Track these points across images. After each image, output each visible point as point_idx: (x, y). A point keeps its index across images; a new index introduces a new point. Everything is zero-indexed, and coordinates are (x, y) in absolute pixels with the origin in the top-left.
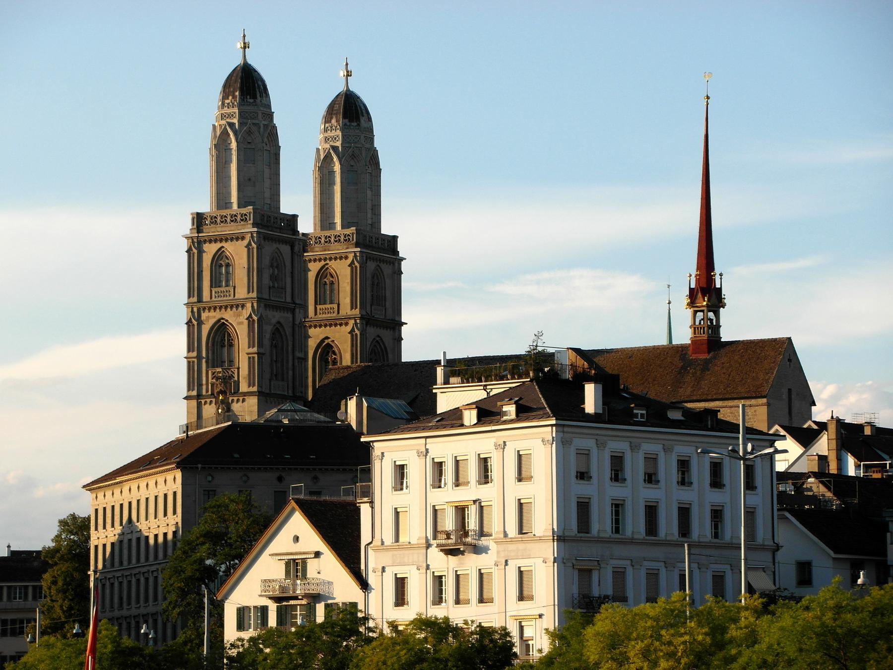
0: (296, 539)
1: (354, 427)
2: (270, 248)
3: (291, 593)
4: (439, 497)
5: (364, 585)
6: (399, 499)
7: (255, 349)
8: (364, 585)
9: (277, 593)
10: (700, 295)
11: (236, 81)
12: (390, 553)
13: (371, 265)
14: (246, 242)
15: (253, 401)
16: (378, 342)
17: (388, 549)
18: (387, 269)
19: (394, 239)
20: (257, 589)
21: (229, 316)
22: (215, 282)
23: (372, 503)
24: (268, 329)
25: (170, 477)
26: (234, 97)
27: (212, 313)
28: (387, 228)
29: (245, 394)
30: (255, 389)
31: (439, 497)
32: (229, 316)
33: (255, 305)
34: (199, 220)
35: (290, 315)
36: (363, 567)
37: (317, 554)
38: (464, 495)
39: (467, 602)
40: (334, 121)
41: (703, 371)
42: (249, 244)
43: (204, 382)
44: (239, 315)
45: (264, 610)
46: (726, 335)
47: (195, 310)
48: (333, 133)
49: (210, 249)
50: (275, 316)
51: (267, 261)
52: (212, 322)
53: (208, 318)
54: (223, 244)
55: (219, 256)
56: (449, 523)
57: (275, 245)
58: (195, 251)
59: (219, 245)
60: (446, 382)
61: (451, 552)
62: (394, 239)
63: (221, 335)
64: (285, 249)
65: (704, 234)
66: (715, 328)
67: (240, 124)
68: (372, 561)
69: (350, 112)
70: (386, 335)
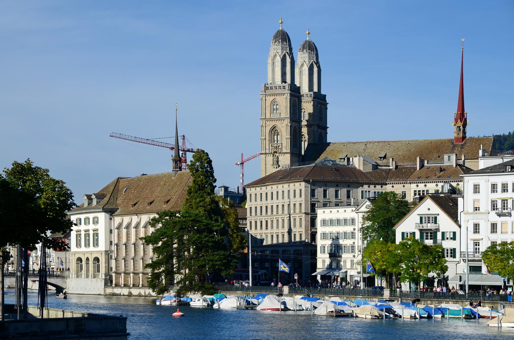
0: (429, 209)
1: (358, 168)
2: (294, 98)
3: (425, 228)
4: (494, 196)
5: (460, 226)
6: (477, 196)
7: (289, 137)
8: (460, 226)
9: (421, 228)
10: (459, 120)
11: (279, 36)
12: (472, 215)
13: (319, 105)
14: (285, 97)
15: (289, 156)
16: (321, 134)
17: (470, 214)
18: (323, 107)
19: (325, 95)
20: (414, 225)
21: (278, 123)
22: (273, 110)
23: (463, 197)
24: (292, 129)
25: (297, 184)
26: (279, 42)
27: (271, 122)
28: (323, 92)
29: (285, 153)
30: (289, 151)
31: (494, 196)
32: (278, 123)
33: (289, 120)
34: (266, 88)
35: (298, 124)
36: (459, 219)
37: (438, 215)
38: (505, 195)
39: (507, 233)
40: (305, 51)
41: (461, 148)
42: (287, 97)
43: (267, 147)
44: (282, 123)
45: (414, 233)
46: (468, 135)
47: (264, 121)
48: (304, 55)
49: (270, 99)
50: (294, 124)
51: (292, 103)
52: (271, 126)
53: (269, 125)
54: (275, 97)
55: (273, 102)
56: (499, 205)
57: (294, 98)
58: (264, 99)
59: (273, 97)
60: (483, 156)
61: (499, 215)
62: (325, 95)
63: (274, 131)
64: (297, 99)
65: (461, 98)
66: (464, 133)
67: (282, 52)
68: (462, 218)
69: (311, 47)
70: (322, 131)
